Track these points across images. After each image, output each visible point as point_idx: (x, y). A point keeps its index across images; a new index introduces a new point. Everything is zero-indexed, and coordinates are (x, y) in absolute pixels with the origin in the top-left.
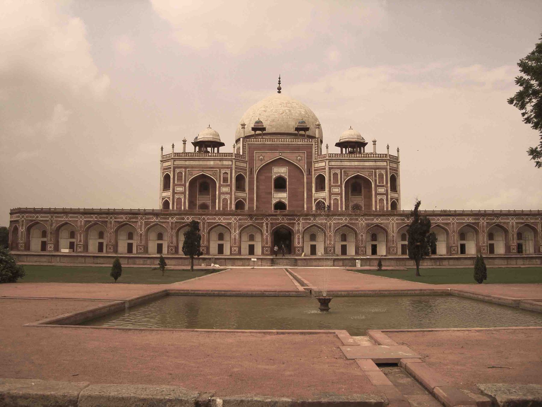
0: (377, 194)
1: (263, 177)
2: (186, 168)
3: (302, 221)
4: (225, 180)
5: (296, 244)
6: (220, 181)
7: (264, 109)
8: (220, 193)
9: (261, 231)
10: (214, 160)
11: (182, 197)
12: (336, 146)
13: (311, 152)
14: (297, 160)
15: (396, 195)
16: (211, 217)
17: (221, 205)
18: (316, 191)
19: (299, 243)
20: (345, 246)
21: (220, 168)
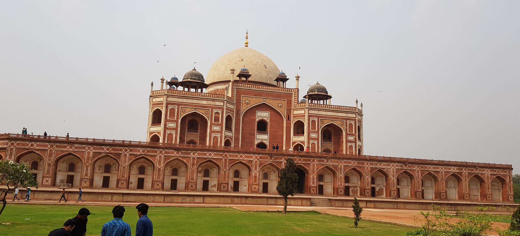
0: (347, 141)
2: (179, 104)
4: (217, 119)
5: (311, 184)
6: (211, 119)
8: (211, 132)
10: (207, 100)
11: (173, 132)
13: (291, 101)
14: (278, 106)
15: (360, 144)
19: (313, 183)
21: (212, 108)
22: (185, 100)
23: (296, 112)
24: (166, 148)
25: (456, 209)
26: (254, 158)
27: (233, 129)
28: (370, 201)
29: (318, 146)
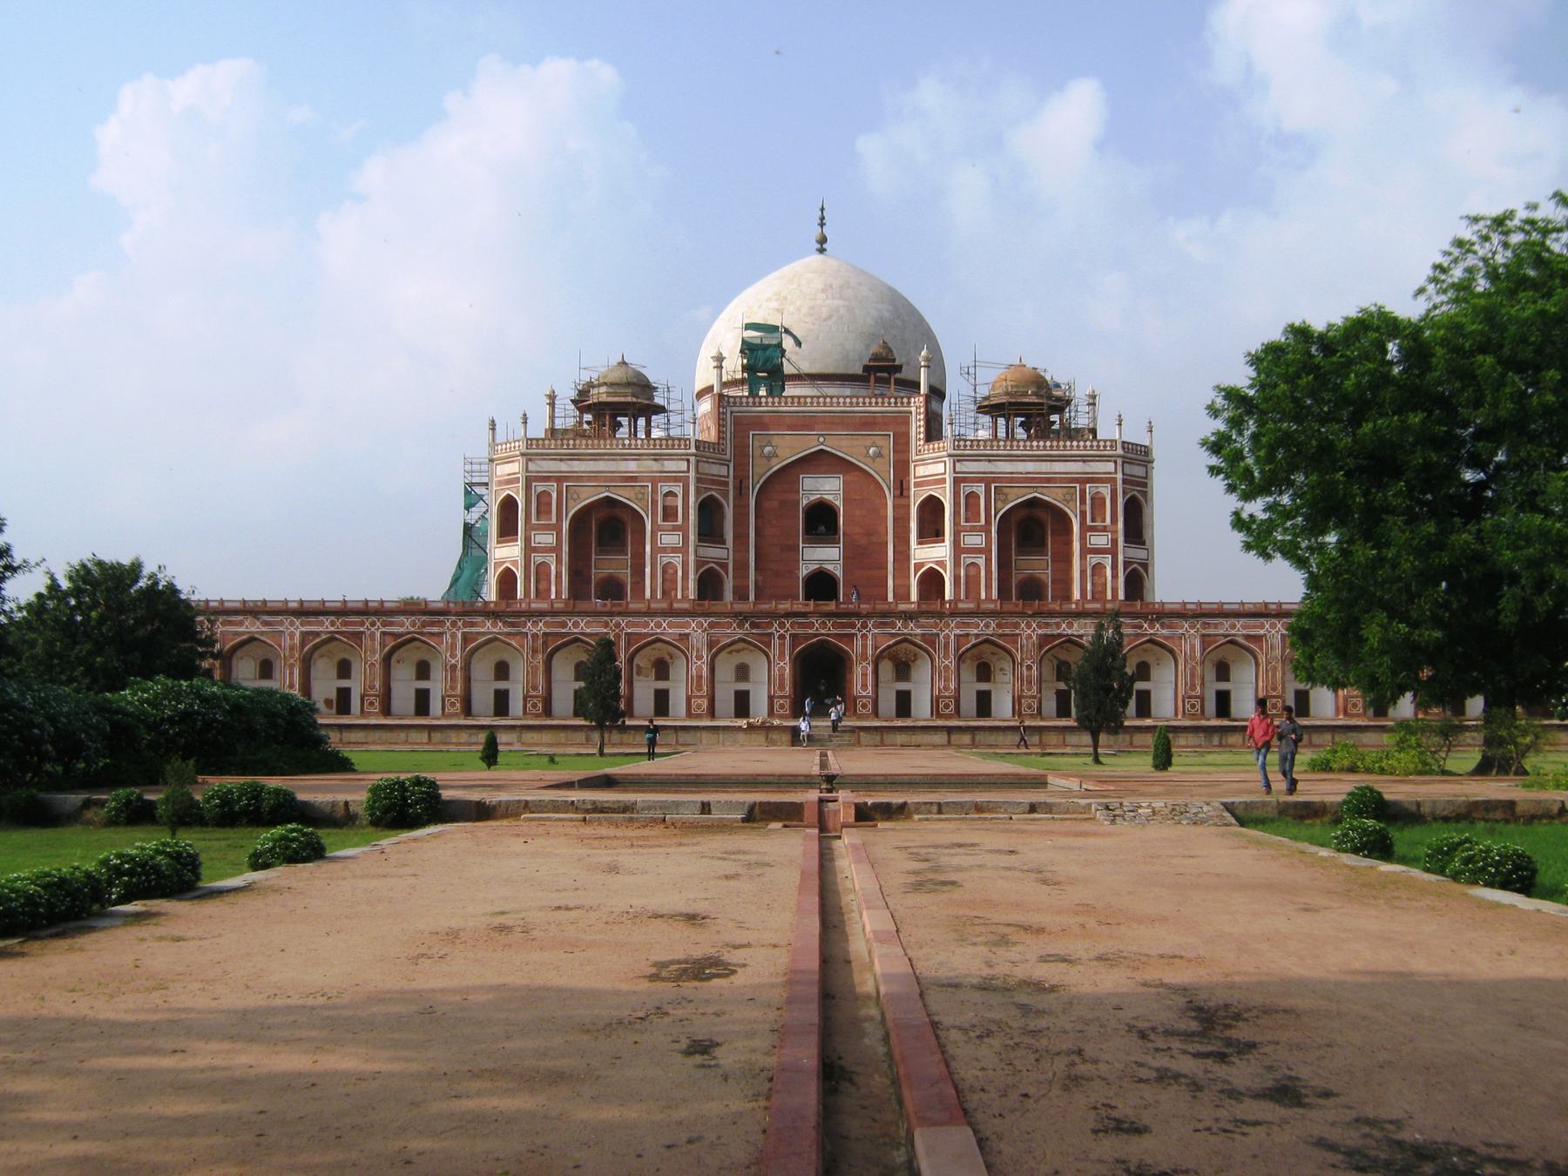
0: (1085, 551)
1: (771, 504)
2: (559, 480)
4: (669, 513)
6: (654, 514)
7: (776, 305)
8: (654, 550)
11: (551, 560)
13: (907, 435)
15: (1139, 554)
16: (636, 620)
17: (660, 580)
18: (920, 543)
19: (864, 686)
21: (654, 481)
22: (577, 466)
23: (922, 471)
24: (465, 613)
27: (729, 535)
28: (959, 729)
29: (988, 572)
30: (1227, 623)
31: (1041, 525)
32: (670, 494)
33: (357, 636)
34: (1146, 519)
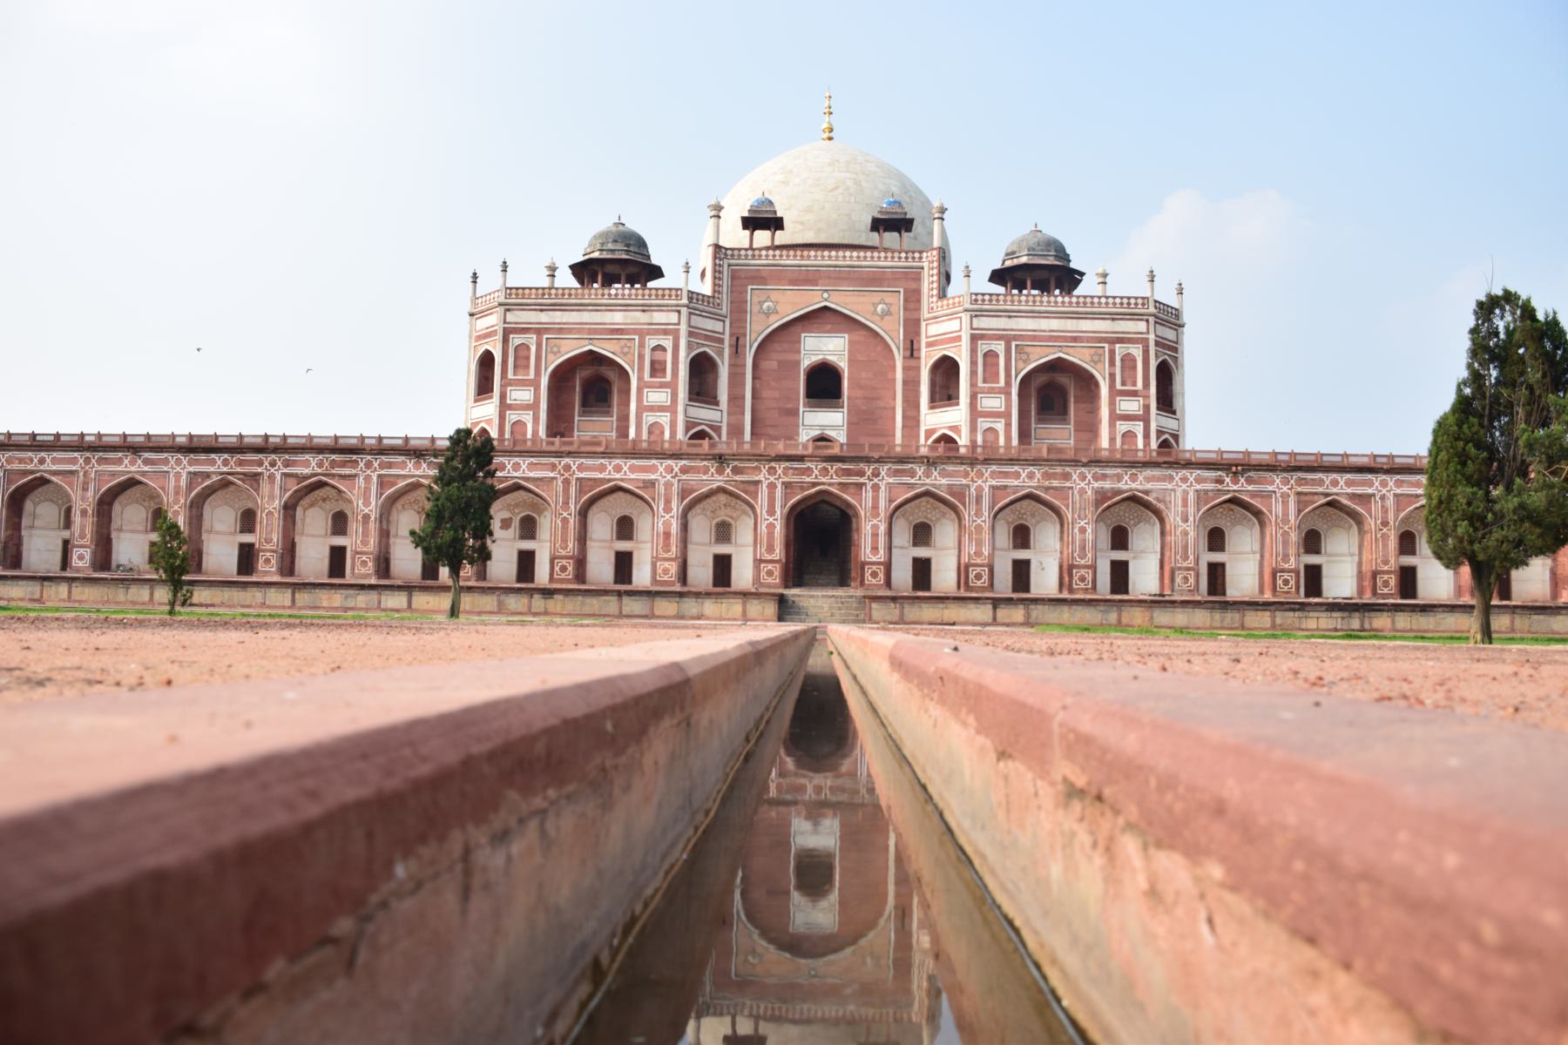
0: (1115, 417)
1: (770, 364)
2: (539, 332)
3: (886, 479)
4: (657, 368)
6: (641, 369)
8: (641, 409)
9: (752, 507)
10: (626, 308)
11: (527, 417)
12: (991, 280)
15: (1170, 423)
16: (589, 462)
19: (875, 549)
20: (1027, 563)
21: (642, 334)
25: (1367, 626)
26: (662, 473)
30: (1328, 478)
31: (1063, 393)
32: (659, 348)
33: (255, 478)
34: (1176, 387)
